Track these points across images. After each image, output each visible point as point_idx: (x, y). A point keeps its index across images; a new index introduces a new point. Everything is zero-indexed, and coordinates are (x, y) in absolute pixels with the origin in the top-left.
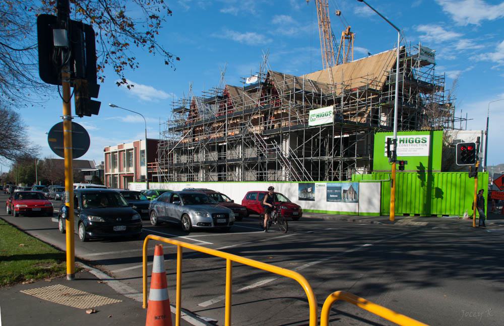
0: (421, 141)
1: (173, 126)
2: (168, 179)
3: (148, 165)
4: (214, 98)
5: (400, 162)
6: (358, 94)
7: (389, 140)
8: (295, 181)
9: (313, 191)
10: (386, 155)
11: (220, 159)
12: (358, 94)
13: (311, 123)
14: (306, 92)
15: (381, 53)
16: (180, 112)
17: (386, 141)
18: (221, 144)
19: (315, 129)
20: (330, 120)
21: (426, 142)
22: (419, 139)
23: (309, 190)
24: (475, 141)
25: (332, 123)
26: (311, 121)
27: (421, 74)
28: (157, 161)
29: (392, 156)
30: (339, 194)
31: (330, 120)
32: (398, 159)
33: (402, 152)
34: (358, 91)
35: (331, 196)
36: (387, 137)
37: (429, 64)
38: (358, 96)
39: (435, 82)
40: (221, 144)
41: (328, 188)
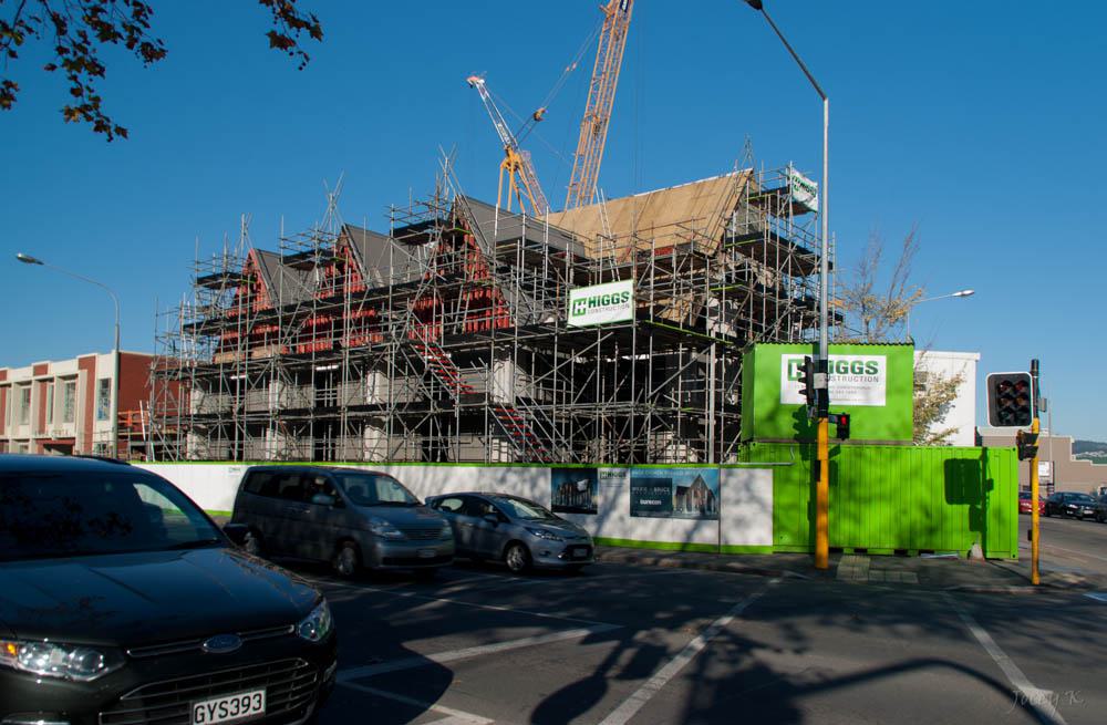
0: (865, 368)
1: (195, 321)
2: (174, 455)
3: (119, 417)
4: (313, 252)
5: (839, 417)
6: (674, 259)
11: (320, 404)
12: (674, 259)
13: (574, 321)
14: (552, 250)
15: (701, 181)
16: (213, 287)
18: (324, 368)
19: (583, 338)
20: (626, 312)
21: (876, 371)
22: (860, 363)
23: (581, 485)
25: (630, 322)
26: (574, 314)
28: (145, 408)
30: (667, 500)
31: (626, 312)
32: (830, 410)
34: (674, 255)
35: (642, 502)
38: (674, 265)
40: (324, 368)
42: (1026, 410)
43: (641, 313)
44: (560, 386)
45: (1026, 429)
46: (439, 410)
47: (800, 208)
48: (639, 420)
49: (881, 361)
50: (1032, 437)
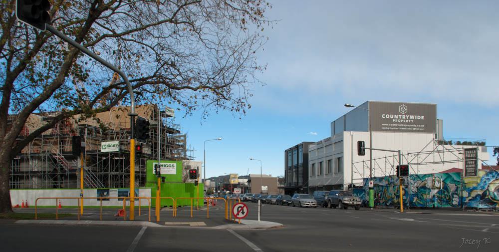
7: (156, 165)
8: (92, 188)
9: (108, 194)
10: (154, 173)
13: (102, 151)
17: (154, 166)
19: (106, 154)
23: (105, 194)
24: (196, 169)
27: (167, 122)
29: (158, 174)
31: (117, 149)
33: (164, 171)
36: (154, 164)
37: (171, 117)
39: (175, 128)
41: (119, 192)
42: (196, 176)
43: (121, 150)
44: (99, 166)
45: (196, 180)
46: (61, 173)
47: (168, 116)
48: (121, 176)
49: (175, 164)
50: (198, 181)
